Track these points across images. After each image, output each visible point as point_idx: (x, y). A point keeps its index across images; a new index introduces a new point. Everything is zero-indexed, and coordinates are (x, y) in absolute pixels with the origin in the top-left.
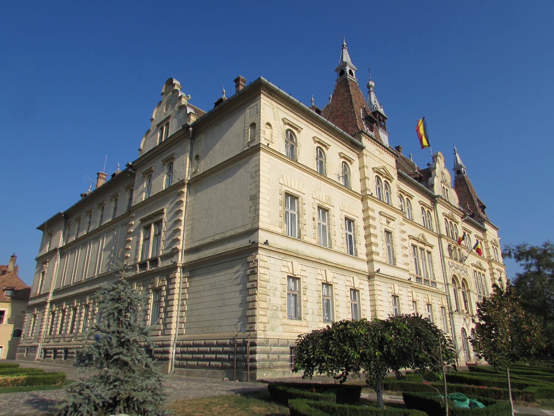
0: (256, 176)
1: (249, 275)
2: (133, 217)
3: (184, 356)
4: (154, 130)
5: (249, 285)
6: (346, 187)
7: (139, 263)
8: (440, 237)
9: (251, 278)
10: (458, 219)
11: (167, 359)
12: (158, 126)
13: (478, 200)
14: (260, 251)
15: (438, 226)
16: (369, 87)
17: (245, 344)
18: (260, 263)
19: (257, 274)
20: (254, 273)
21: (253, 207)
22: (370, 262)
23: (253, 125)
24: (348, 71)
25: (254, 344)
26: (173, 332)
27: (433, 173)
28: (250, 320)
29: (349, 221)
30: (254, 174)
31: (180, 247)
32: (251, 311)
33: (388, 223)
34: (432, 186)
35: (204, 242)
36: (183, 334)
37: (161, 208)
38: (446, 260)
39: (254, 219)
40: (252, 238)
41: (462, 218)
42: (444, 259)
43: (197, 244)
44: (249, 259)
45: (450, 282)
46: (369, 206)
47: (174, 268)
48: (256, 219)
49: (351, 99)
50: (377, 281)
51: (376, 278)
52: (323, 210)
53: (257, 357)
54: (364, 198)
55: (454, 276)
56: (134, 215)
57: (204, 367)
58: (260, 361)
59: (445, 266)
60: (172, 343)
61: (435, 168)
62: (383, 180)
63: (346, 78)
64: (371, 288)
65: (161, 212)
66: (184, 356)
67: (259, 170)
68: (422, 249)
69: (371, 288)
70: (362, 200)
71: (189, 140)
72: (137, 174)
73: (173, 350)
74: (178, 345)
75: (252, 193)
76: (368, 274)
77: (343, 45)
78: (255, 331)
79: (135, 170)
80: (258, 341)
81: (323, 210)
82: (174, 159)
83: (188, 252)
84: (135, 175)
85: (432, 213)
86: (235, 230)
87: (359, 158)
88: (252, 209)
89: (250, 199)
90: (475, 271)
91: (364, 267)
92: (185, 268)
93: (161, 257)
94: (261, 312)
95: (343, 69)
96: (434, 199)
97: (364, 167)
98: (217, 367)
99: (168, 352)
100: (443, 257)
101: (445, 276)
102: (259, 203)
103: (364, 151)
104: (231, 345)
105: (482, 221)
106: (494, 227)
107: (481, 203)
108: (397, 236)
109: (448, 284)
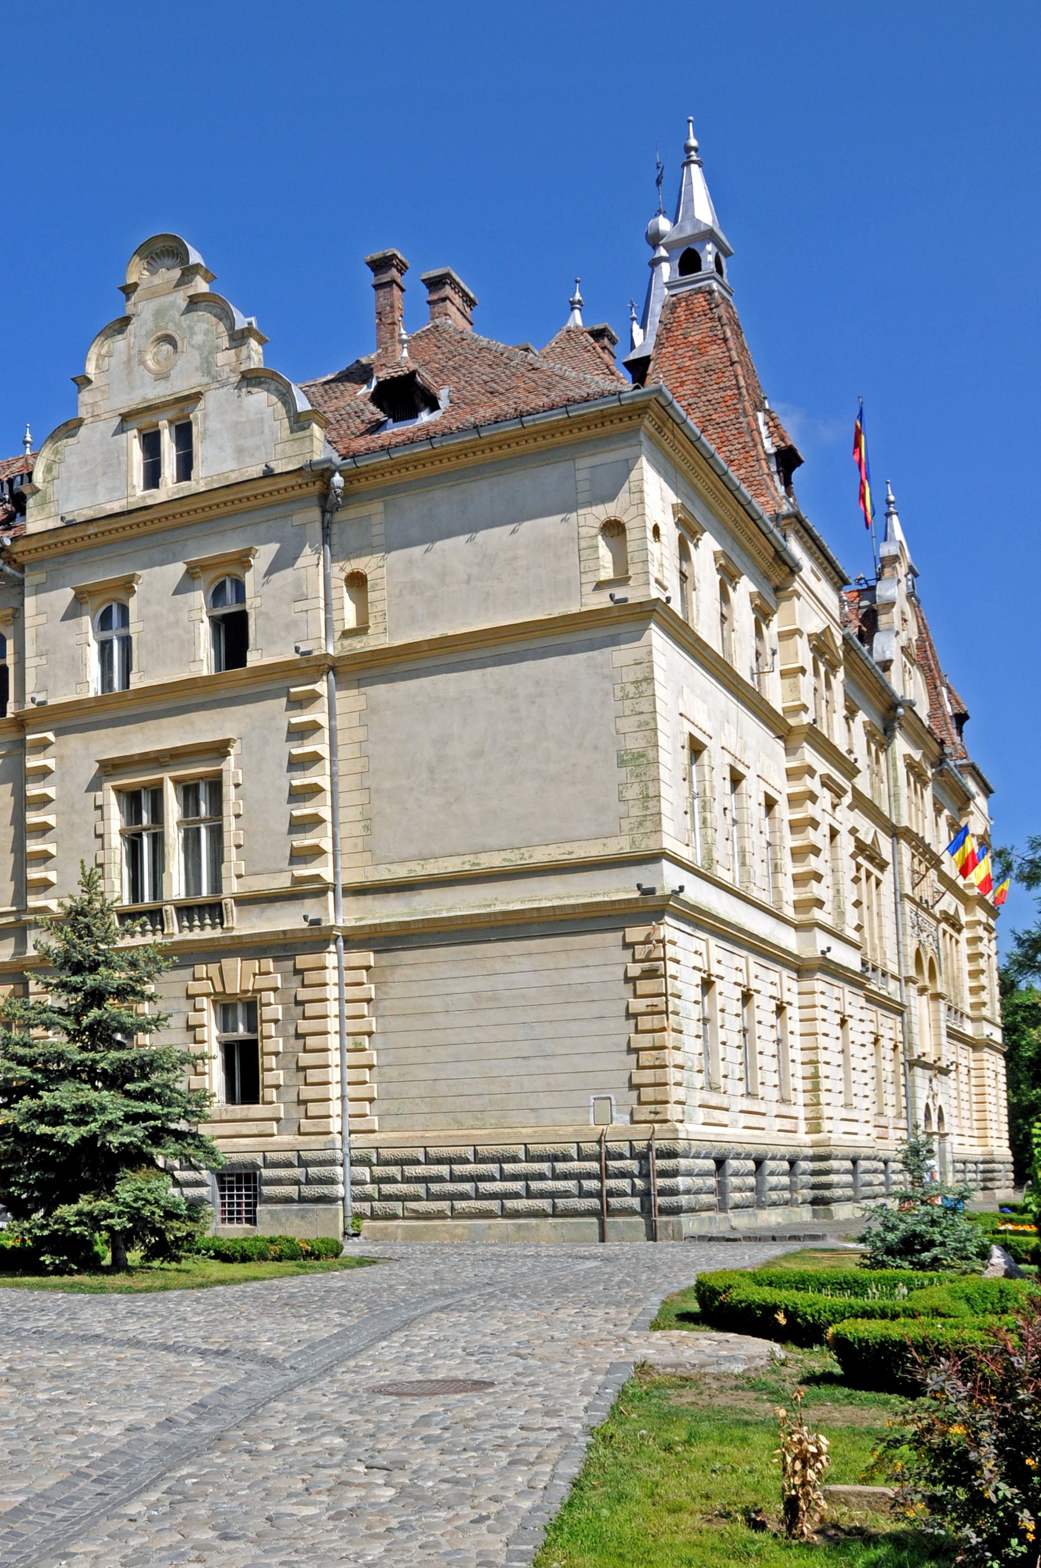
0: (641, 695)
12: (126, 419)
15: (894, 797)
29: (770, 804)
30: (631, 689)
33: (834, 806)
35: (434, 868)
39: (641, 824)
43: (400, 872)
45: (912, 972)
48: (649, 826)
52: (736, 779)
65: (220, 749)
67: (650, 679)
68: (869, 875)
75: (634, 743)
84: (21, 583)
86: (568, 847)
88: (633, 792)
89: (622, 763)
90: (945, 932)
106: (987, 790)
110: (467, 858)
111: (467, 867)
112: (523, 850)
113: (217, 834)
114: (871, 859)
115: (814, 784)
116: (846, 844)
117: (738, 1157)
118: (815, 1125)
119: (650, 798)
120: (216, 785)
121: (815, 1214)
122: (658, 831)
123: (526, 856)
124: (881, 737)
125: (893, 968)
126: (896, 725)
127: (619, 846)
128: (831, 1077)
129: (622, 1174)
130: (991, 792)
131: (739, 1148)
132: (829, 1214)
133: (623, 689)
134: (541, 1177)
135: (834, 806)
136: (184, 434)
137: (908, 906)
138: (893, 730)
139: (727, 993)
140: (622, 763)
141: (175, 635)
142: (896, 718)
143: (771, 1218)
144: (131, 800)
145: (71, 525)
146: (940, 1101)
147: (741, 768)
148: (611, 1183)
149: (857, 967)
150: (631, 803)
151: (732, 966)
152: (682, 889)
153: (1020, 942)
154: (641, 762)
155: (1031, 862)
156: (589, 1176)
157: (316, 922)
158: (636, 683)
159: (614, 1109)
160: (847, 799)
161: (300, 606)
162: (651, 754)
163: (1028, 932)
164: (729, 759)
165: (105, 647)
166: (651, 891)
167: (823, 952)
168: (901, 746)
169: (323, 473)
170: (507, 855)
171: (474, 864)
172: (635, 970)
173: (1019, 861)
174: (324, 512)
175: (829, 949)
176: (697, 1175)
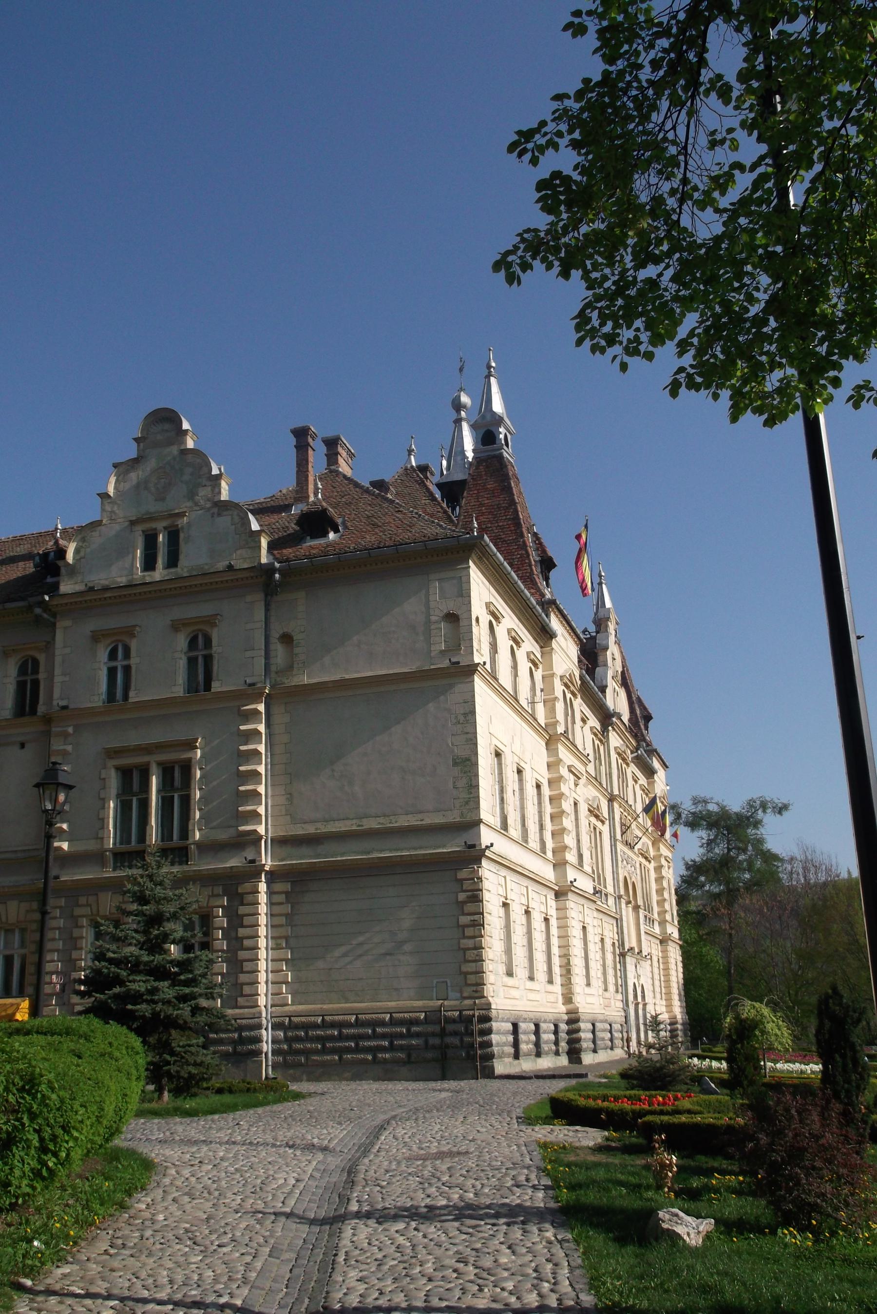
1: (464, 903)
2: (66, 735)
3: (298, 1046)
4: (117, 527)
5: (464, 920)
6: (530, 718)
7: (110, 850)
8: (611, 799)
9: (469, 908)
10: (630, 756)
11: (259, 1053)
13: (639, 699)
14: (484, 863)
16: (458, 406)
17: (469, 1020)
18: (486, 884)
19: (482, 901)
20: (476, 897)
21: (464, 781)
22: (560, 865)
23: (453, 618)
24: (502, 436)
25: (488, 1019)
26: (262, 1001)
27: (601, 659)
28: (471, 979)
30: (462, 718)
31: (261, 829)
32: (474, 964)
33: (576, 785)
34: (603, 689)
36: (287, 1005)
37: (178, 733)
38: (620, 846)
40: (468, 837)
41: (632, 752)
42: (615, 845)
43: (311, 829)
44: (463, 874)
46: (561, 756)
47: (254, 871)
49: (516, 511)
50: (573, 903)
51: (570, 896)
52: (519, 772)
53: (495, 1038)
54: (551, 740)
55: (625, 878)
56: (70, 730)
57: (364, 1061)
58: (498, 1045)
59: (617, 860)
60: (264, 1022)
61: (606, 648)
62: (569, 696)
63: (501, 457)
64: (561, 913)
65: (191, 745)
66: (298, 1046)
67: (473, 712)
69: (561, 915)
70: (547, 744)
71: (260, 596)
72: (58, 625)
73: (266, 1035)
74: (276, 1027)
75: (462, 752)
76: (557, 888)
77: (489, 367)
78: (484, 997)
79: (54, 615)
80: (493, 1013)
81: (519, 772)
82: (214, 625)
83: (279, 842)
85: (602, 748)
87: (542, 654)
88: (462, 783)
89: (455, 764)
91: (548, 873)
92: (273, 877)
93: (198, 845)
94: (491, 968)
95: (493, 429)
96: (606, 717)
97: (553, 675)
98: (395, 1061)
99: (259, 1040)
100: (615, 840)
101: (615, 879)
102: (477, 775)
103: (554, 643)
104: (426, 1021)
105: (652, 752)
106: (665, 766)
107: (645, 709)
108: (583, 809)
109: (620, 897)
110: (354, 821)
111: (354, 828)
112: (391, 817)
113: (186, 801)
114: (597, 817)
115: (564, 771)
116: (583, 809)
117: (525, 1020)
118: (568, 999)
119: (473, 787)
120: (187, 768)
121: (570, 1061)
122: (478, 807)
123: (393, 821)
124: (602, 735)
125: (610, 889)
126: (610, 728)
127: (453, 817)
128: (577, 963)
129: (455, 1033)
130: (667, 767)
131: (525, 1015)
132: (579, 1061)
133: (456, 717)
134: (401, 1036)
135: (576, 785)
136: (174, 536)
137: (620, 846)
138: (608, 731)
139: (517, 913)
140: (455, 764)
141: (160, 670)
142: (612, 724)
143: (546, 1063)
144: (125, 773)
145: (91, 589)
146: (642, 981)
147: (522, 764)
148: (449, 1040)
149: (592, 892)
150: (461, 790)
151: (518, 892)
152: (492, 845)
153: (688, 867)
154: (467, 765)
155: (693, 814)
156: (433, 1034)
157: (253, 861)
158: (465, 715)
159: (449, 989)
160: (583, 781)
161: (249, 654)
162: (473, 759)
163: (694, 861)
164: (516, 759)
165: (112, 672)
166: (473, 846)
167: (571, 882)
168: (615, 740)
169: (269, 570)
170: (381, 820)
171: (359, 826)
172: (462, 896)
173: (686, 812)
174: (266, 595)
175: (575, 880)
176: (503, 1033)
